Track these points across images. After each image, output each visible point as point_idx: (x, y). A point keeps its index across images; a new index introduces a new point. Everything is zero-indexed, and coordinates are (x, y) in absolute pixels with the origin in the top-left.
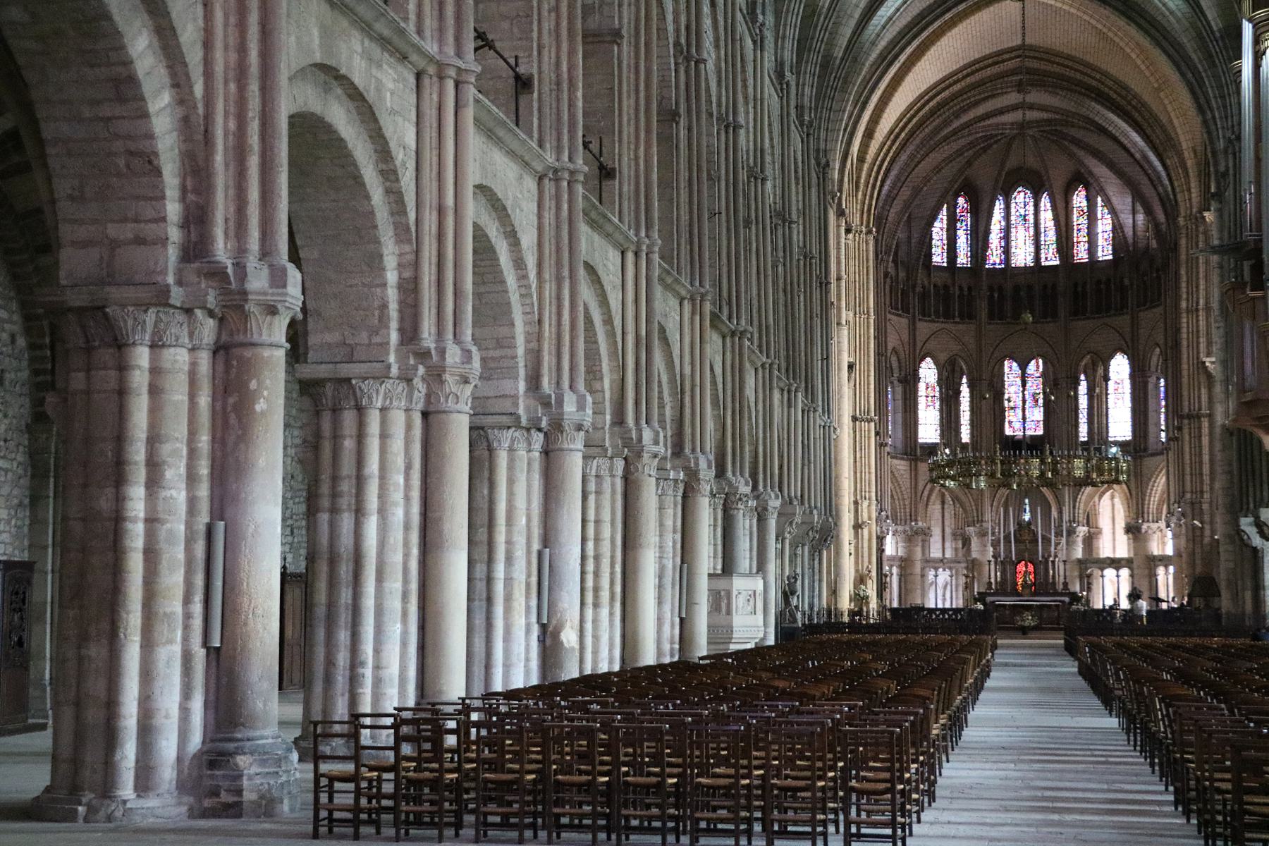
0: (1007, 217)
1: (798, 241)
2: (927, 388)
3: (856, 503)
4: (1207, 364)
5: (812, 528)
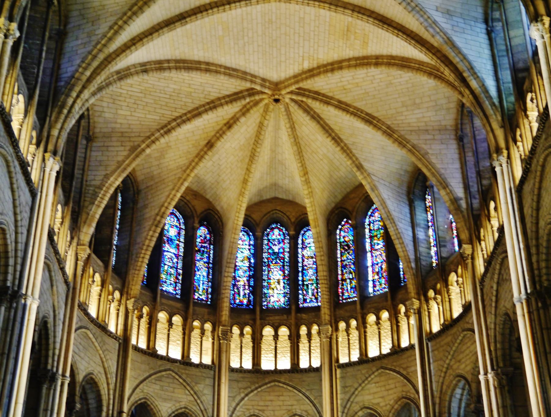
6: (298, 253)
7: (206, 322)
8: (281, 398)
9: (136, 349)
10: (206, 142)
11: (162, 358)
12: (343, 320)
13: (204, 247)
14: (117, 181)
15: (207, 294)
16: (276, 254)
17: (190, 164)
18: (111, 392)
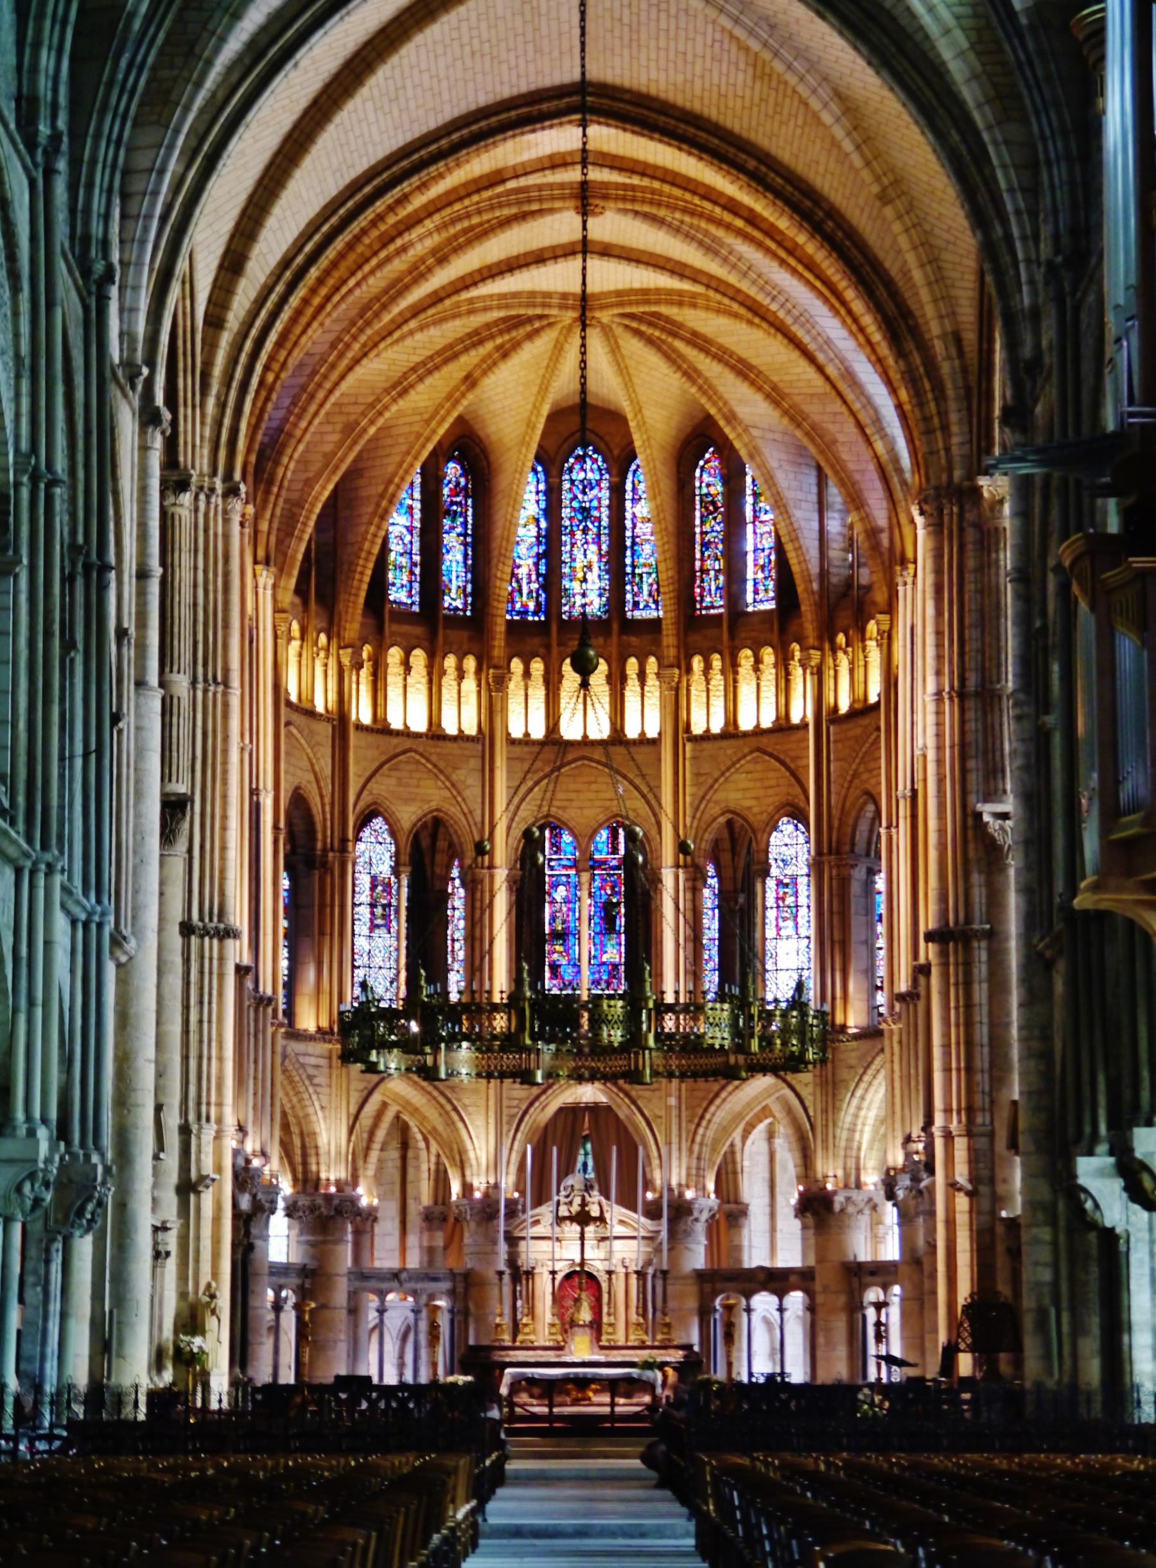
0: (552, 509)
1: (17, 437)
2: (373, 888)
3: (185, 1130)
4: (986, 818)
5: (32, 1176)
6: (624, 510)
7: (466, 654)
8: (594, 787)
9: (359, 727)
10: (464, 374)
11: (398, 733)
12: (700, 654)
13: (456, 503)
14: (324, 491)
15: (466, 596)
16: (585, 512)
17: (436, 412)
18: (328, 808)
